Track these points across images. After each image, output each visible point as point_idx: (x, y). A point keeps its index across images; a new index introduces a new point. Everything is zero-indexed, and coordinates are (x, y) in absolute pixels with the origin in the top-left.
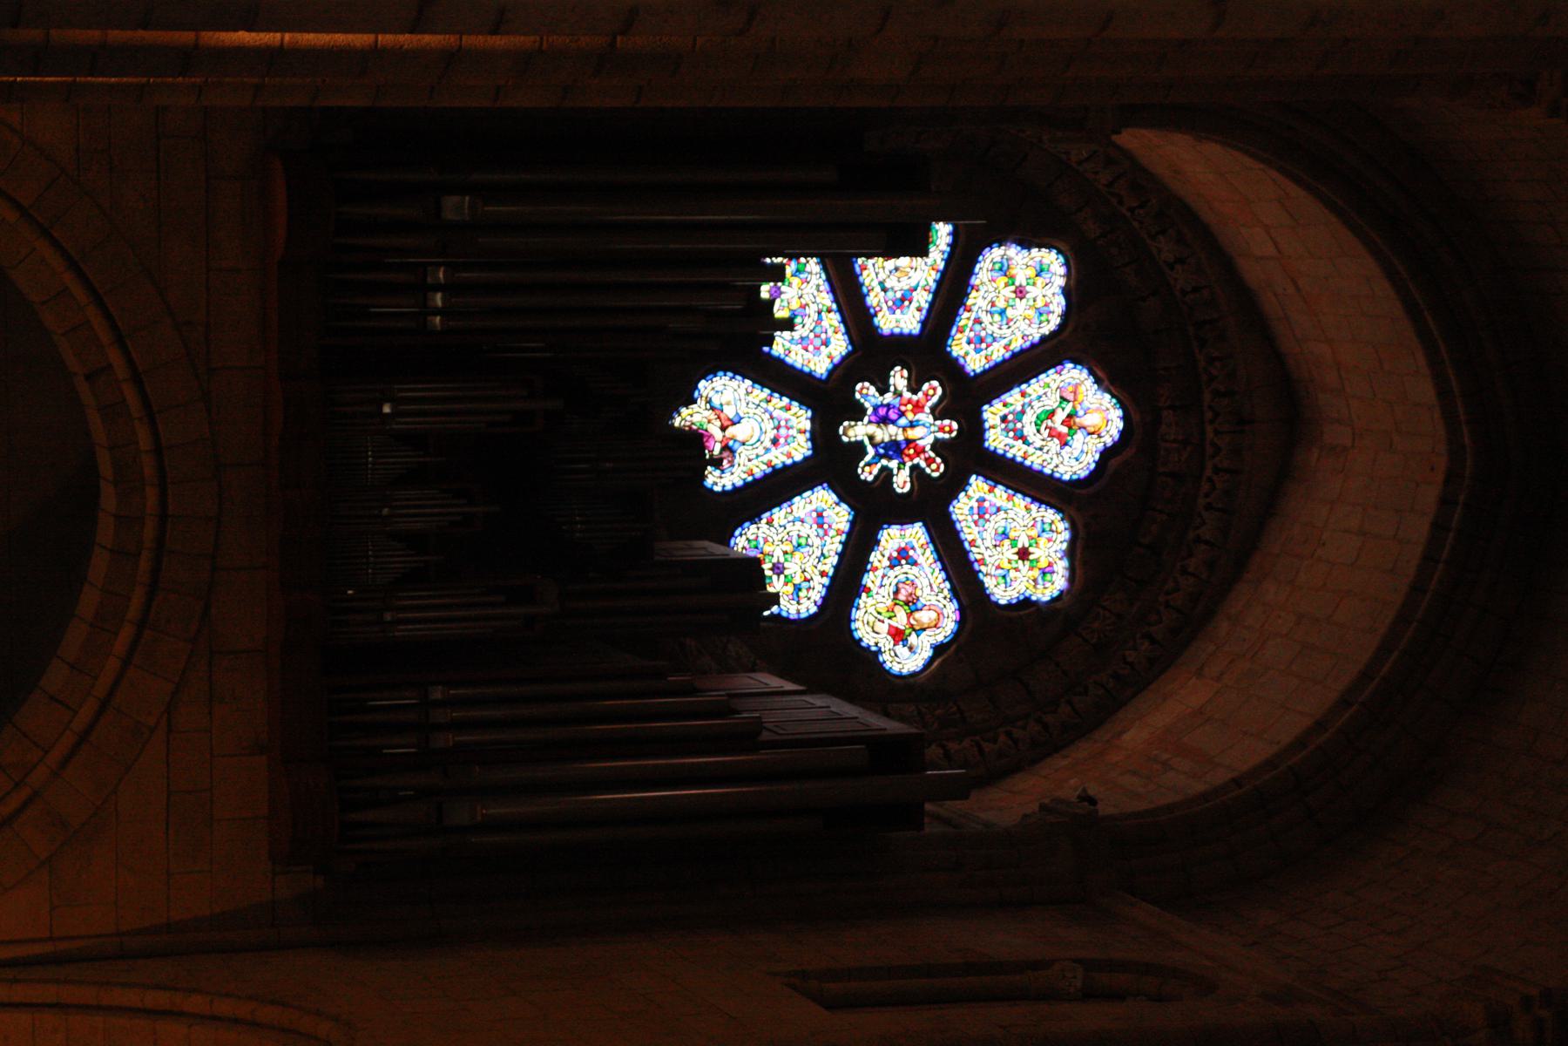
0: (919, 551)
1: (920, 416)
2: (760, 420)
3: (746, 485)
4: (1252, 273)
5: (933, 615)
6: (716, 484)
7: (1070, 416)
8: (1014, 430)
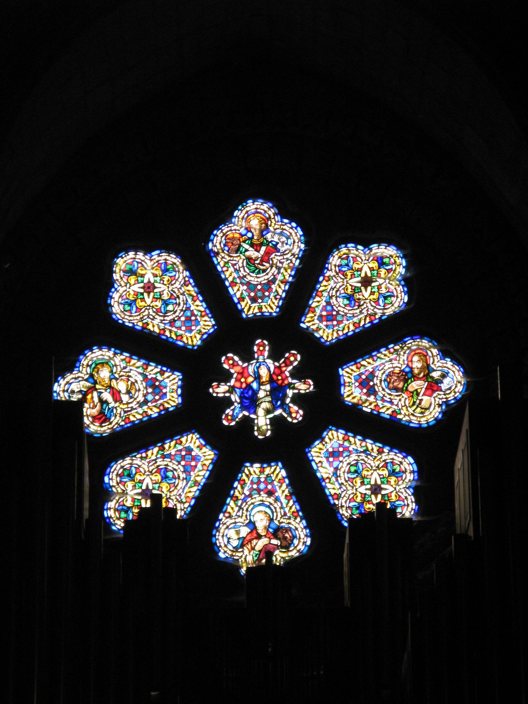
0: (362, 370)
2: (252, 506)
5: (416, 358)
6: (304, 543)
7: (252, 245)
8: (263, 290)
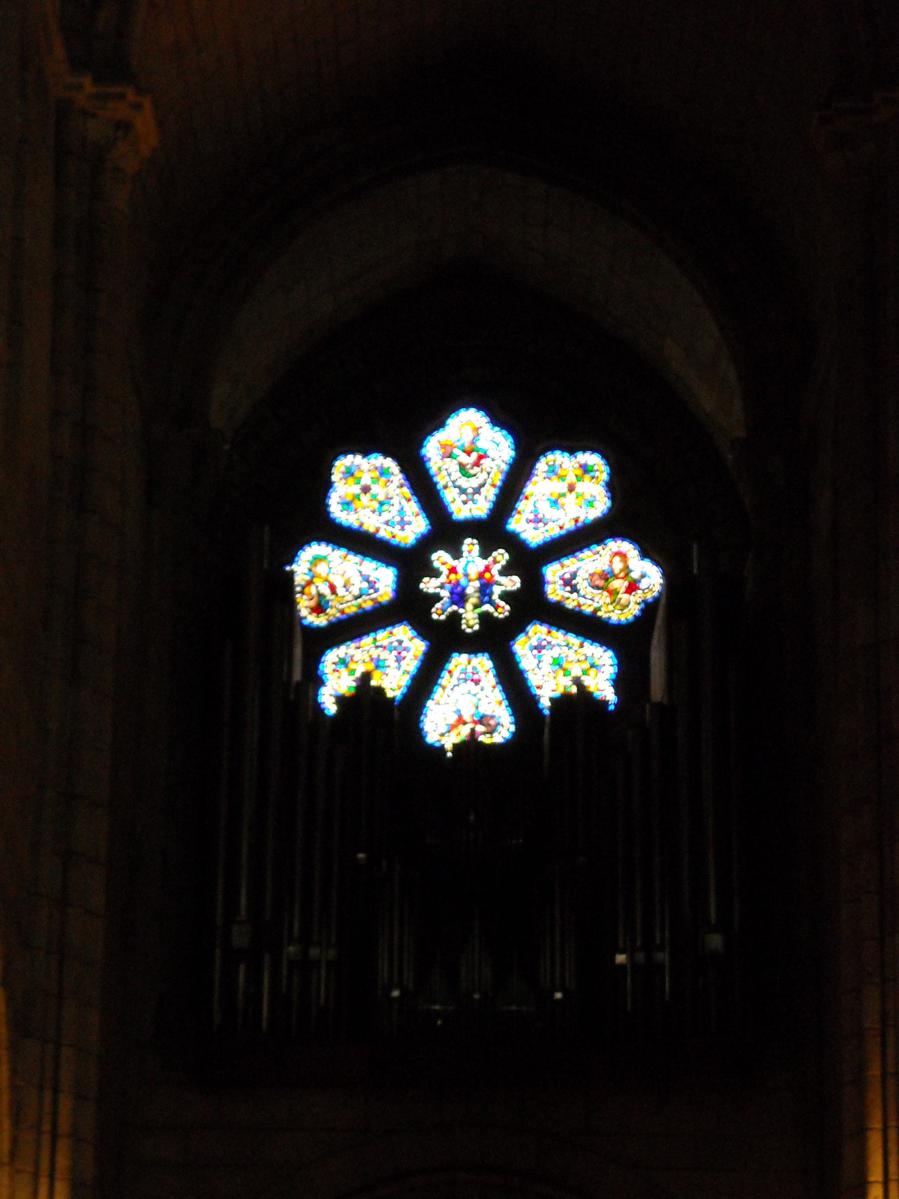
1: (460, 569)
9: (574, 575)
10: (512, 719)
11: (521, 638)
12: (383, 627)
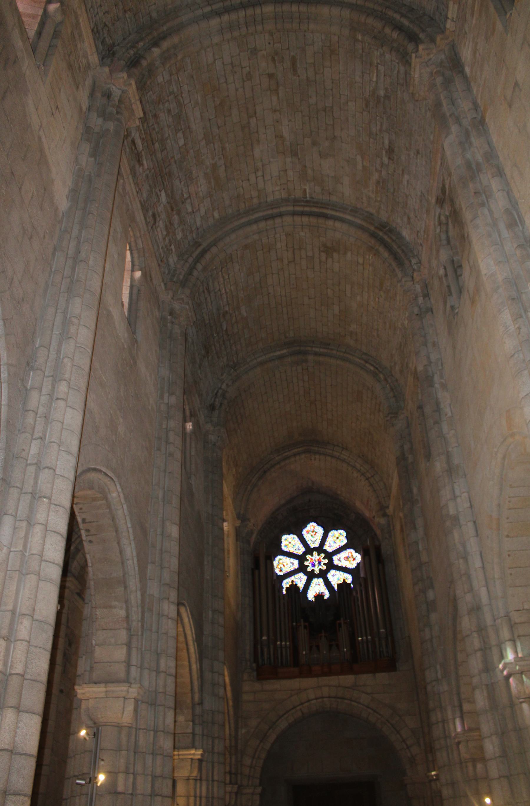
1: (313, 559)
3: (328, 589)
4: (283, 502)
9: (340, 558)
10: (329, 593)
11: (329, 573)
12: (296, 574)
